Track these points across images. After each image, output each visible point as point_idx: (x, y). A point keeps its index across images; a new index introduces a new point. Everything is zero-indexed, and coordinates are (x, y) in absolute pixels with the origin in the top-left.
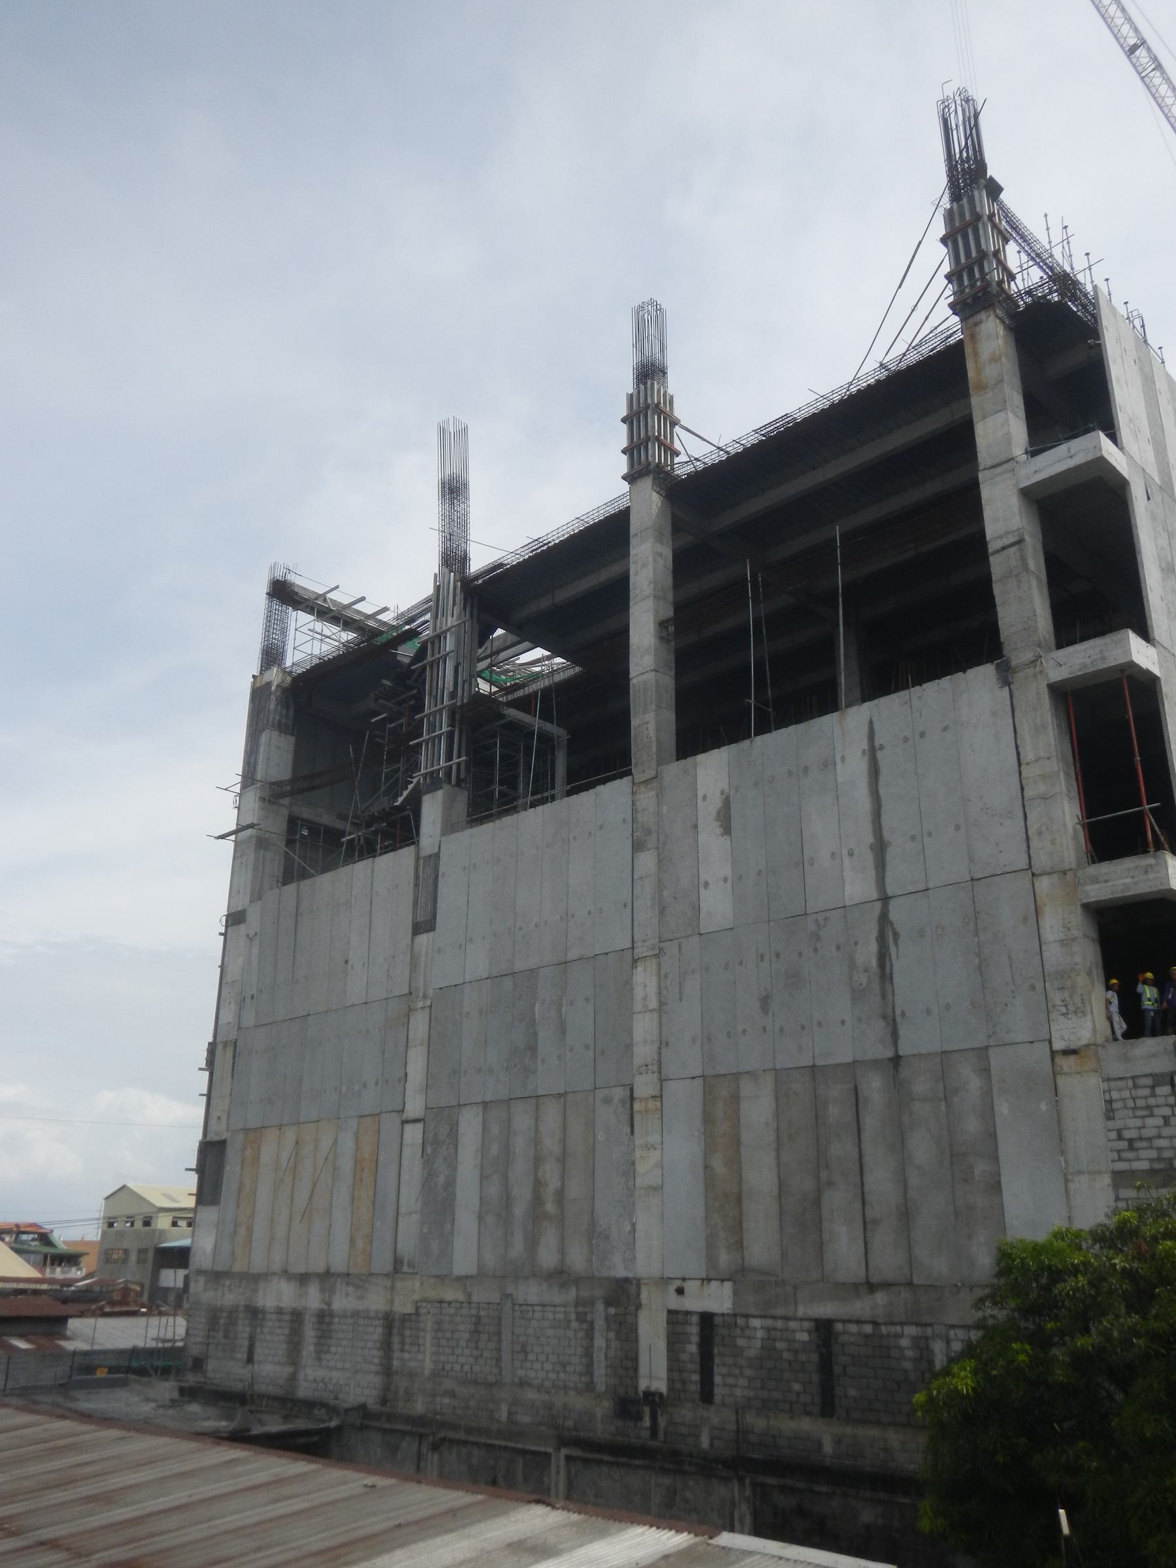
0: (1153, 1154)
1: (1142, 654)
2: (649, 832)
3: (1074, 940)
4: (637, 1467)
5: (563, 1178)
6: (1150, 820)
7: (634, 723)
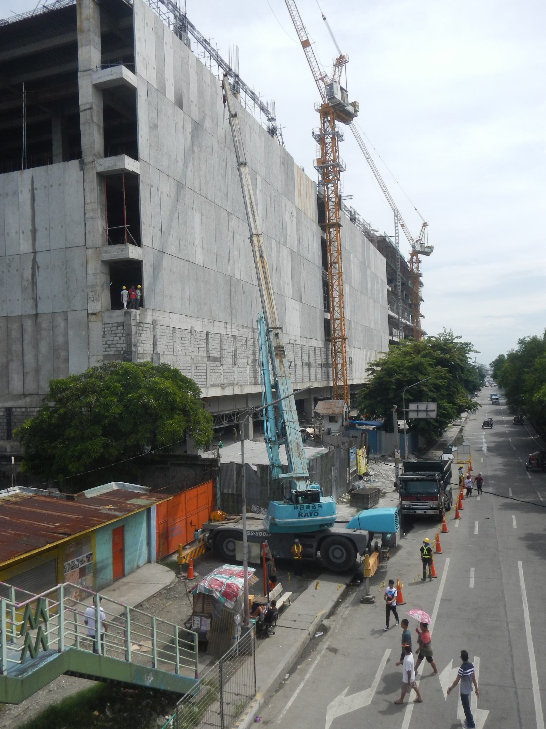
0: (115, 349)
3: (97, 274)
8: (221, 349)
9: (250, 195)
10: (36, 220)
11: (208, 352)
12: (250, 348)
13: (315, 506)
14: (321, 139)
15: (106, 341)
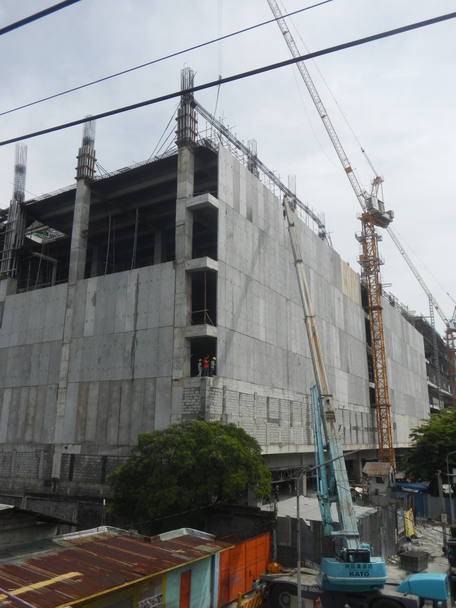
0: (192, 409)
1: (210, 263)
2: (71, 302)
4: (48, 500)
5: (35, 413)
7: (71, 265)
8: (280, 412)
9: (305, 286)
10: (138, 305)
11: (268, 414)
12: (304, 412)
13: (365, 566)
14: (363, 240)
15: (185, 403)
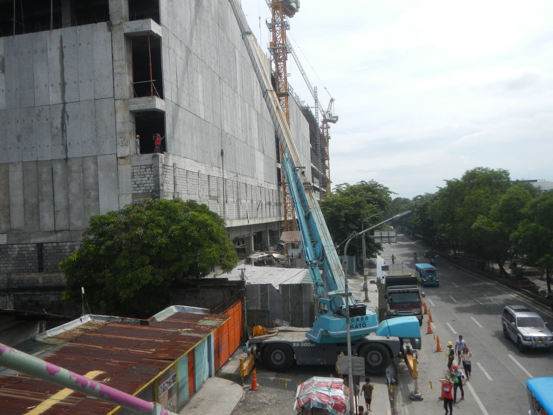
0: (144, 188)
1: (154, 27)
6: (153, 85)
11: (209, 192)
12: (235, 189)
13: (362, 318)
14: (272, 27)
